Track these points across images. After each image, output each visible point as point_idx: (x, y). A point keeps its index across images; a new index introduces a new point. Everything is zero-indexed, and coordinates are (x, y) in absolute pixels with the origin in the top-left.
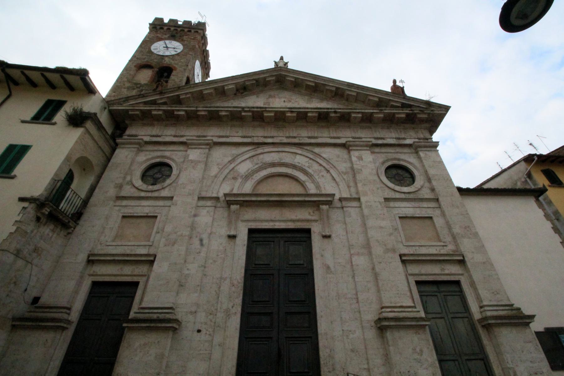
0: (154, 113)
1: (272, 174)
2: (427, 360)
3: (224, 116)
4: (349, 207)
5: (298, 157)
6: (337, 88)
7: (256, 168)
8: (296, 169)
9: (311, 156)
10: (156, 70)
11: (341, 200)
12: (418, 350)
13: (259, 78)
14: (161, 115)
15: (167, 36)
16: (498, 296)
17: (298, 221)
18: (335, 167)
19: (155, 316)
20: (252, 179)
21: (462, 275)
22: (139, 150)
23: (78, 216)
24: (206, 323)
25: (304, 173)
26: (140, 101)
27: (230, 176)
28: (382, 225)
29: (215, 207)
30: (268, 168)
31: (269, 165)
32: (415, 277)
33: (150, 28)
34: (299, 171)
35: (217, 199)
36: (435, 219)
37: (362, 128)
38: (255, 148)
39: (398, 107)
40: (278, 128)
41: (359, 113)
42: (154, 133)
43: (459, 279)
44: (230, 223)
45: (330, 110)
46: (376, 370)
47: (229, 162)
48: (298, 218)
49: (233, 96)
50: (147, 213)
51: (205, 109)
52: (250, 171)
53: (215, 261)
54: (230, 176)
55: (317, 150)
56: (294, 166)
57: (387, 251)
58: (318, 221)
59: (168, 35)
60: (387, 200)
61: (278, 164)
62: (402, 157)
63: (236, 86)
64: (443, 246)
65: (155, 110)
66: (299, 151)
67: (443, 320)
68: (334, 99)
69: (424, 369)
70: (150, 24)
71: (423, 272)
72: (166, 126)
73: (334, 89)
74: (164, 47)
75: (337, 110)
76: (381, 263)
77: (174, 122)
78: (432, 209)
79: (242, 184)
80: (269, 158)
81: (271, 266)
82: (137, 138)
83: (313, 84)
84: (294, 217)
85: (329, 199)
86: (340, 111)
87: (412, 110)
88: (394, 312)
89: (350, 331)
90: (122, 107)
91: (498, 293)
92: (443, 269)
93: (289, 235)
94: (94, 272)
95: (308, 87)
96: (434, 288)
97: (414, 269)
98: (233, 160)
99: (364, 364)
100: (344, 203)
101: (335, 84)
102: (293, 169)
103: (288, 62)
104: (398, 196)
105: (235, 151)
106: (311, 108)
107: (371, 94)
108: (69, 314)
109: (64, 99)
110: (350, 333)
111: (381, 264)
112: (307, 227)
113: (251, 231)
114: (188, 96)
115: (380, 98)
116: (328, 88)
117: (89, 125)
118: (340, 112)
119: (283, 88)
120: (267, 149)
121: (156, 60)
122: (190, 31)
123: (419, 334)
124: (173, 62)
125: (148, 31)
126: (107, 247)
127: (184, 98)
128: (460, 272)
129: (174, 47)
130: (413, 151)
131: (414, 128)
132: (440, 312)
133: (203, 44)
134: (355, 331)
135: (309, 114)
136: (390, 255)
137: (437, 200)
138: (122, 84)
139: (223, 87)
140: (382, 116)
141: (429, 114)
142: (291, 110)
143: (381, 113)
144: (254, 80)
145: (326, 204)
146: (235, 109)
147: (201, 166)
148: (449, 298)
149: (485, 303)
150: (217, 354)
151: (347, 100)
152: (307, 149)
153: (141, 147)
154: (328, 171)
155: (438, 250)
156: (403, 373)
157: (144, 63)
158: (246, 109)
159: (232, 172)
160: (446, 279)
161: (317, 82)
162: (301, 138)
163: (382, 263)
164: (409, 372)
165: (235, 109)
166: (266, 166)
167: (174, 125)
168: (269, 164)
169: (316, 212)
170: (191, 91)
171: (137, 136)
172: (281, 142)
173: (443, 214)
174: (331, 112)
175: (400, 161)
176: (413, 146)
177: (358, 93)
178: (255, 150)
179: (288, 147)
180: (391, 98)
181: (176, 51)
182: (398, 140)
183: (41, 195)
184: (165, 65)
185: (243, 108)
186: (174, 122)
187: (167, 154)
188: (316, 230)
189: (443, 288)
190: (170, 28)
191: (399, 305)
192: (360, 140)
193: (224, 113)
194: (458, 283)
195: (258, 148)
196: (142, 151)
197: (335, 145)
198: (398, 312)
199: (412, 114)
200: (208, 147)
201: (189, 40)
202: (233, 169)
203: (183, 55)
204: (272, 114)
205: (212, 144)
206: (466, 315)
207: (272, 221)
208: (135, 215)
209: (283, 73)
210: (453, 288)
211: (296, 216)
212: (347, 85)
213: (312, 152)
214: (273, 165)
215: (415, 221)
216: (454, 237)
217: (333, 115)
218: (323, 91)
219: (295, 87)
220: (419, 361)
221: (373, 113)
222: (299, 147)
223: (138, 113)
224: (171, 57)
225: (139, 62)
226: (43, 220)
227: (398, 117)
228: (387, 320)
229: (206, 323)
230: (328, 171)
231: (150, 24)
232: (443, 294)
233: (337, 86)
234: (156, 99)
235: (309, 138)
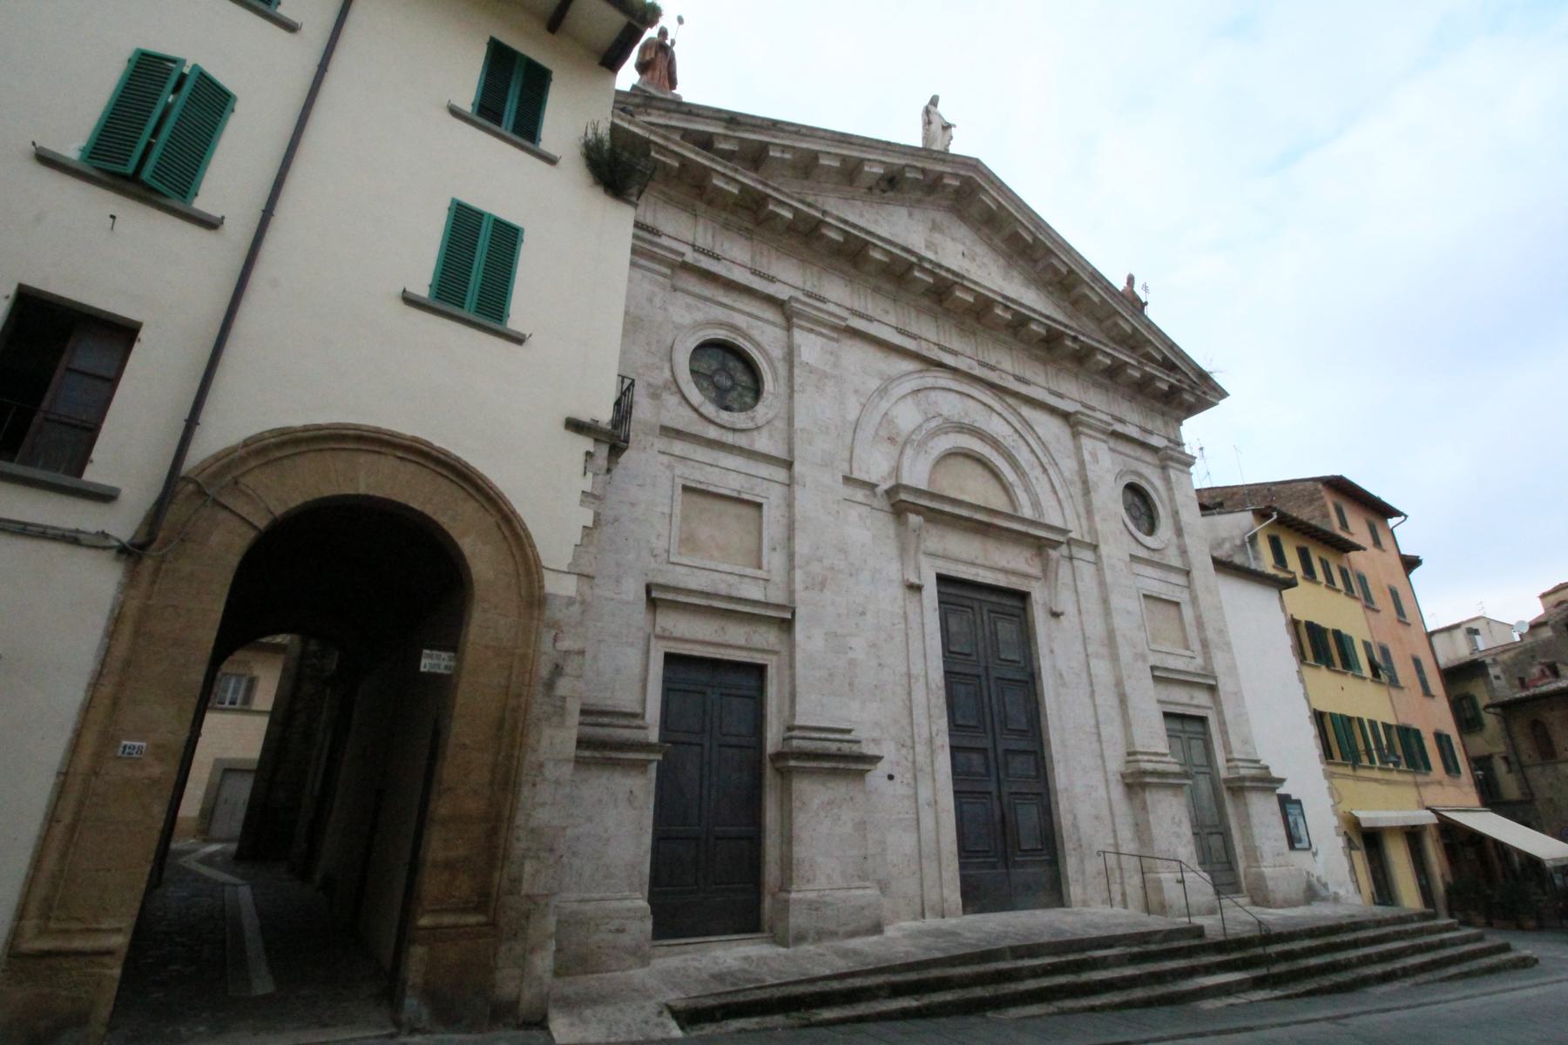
0: (718, 182)
5: (996, 419)
8: (997, 450)
9: (1018, 426)
12: (1177, 820)
18: (1056, 464)
19: (833, 747)
21: (1210, 708)
24: (898, 764)
26: (673, 123)
30: (952, 432)
35: (872, 486)
36: (1183, 607)
38: (921, 371)
40: (961, 330)
41: (1108, 355)
44: (903, 551)
49: (865, 190)
50: (739, 492)
51: (842, 226)
55: (1026, 411)
56: (995, 443)
60: (1133, 558)
61: (968, 429)
65: (723, 175)
66: (997, 406)
68: (1050, 289)
71: (1171, 699)
72: (726, 226)
73: (1064, 270)
82: (656, 239)
83: (1029, 239)
88: (1151, 761)
92: (1192, 698)
93: (994, 598)
94: (664, 630)
98: (882, 392)
103: (955, 126)
106: (1041, 314)
112: (1024, 588)
115: (1135, 329)
116: (1055, 262)
118: (1082, 341)
119: (960, 211)
120: (944, 380)
126: (671, 567)
127: (776, 158)
130: (1157, 462)
131: (1163, 414)
136: (1140, 664)
137: (1188, 573)
140: (1137, 374)
143: (1139, 368)
146: (904, 255)
149: (1236, 755)
151: (1074, 303)
154: (1045, 470)
158: (927, 265)
160: (1193, 713)
165: (904, 255)
167: (748, 234)
169: (1037, 561)
171: (660, 236)
173: (1194, 601)
174: (1068, 335)
176: (1161, 453)
178: (921, 375)
179: (978, 386)
185: (921, 258)
186: (746, 224)
187: (740, 321)
188: (1038, 595)
191: (1153, 750)
193: (877, 255)
194: (1202, 720)
195: (927, 370)
197: (1053, 411)
198: (1156, 762)
206: (1208, 770)
207: (973, 564)
208: (712, 489)
209: (978, 179)
210: (1197, 727)
211: (1008, 562)
214: (995, 444)
216: (1205, 644)
217: (1069, 343)
218: (1036, 261)
221: (1127, 363)
230: (1045, 470)
232: (1187, 735)
233: (1073, 267)
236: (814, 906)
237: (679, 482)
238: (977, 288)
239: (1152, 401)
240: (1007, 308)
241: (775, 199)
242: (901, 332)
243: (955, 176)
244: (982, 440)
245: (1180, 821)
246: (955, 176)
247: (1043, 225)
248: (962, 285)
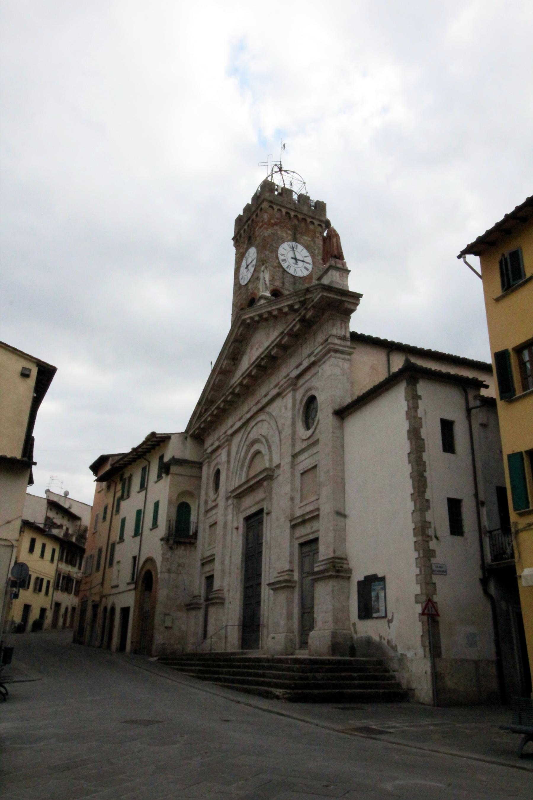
23: (195, 535)
38: (245, 429)
75: (262, 356)
79: (240, 475)
109: (162, 454)
117: (173, 469)
139: (221, 368)
141: (313, 306)
144: (232, 343)
183: (165, 534)
195: (247, 426)
200: (227, 443)
205: (230, 438)
224: (252, 279)
226: (174, 547)
240: (244, 378)
243: (239, 329)
246: (239, 327)
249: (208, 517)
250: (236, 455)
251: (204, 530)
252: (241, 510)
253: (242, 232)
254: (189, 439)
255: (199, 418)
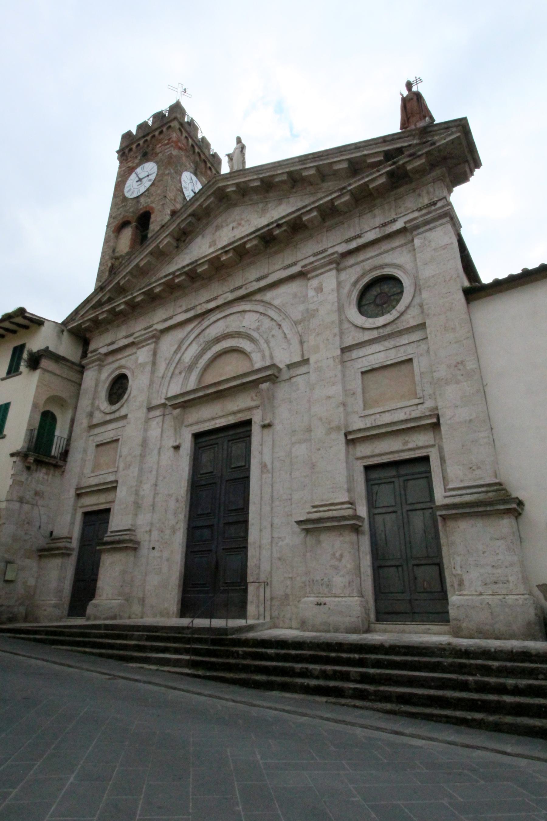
1: (217, 354)
2: (345, 566)
3: (160, 291)
4: (298, 375)
6: (290, 174)
7: (199, 352)
8: (242, 338)
10: (134, 224)
11: (289, 366)
12: (337, 555)
13: (194, 211)
14: (106, 317)
15: (137, 161)
16: (477, 472)
17: (239, 411)
20: (197, 368)
22: (101, 367)
23: (65, 454)
25: (250, 340)
26: (87, 309)
27: (177, 371)
28: (330, 393)
29: (164, 415)
31: (213, 343)
32: (365, 461)
33: (118, 159)
34: (245, 338)
37: (329, 229)
38: (200, 322)
39: (379, 163)
42: (108, 341)
43: (428, 454)
45: (271, 227)
46: (298, 579)
47: (175, 352)
48: (240, 408)
49: (176, 250)
52: (193, 358)
53: (165, 478)
54: (177, 371)
57: (330, 431)
58: (259, 406)
59: (139, 158)
62: (387, 259)
63: (173, 237)
64: (417, 405)
67: (393, 516)
68: (294, 190)
69: (341, 576)
70: (118, 152)
71: (377, 451)
73: (285, 177)
74: (137, 181)
75: (280, 222)
76: (319, 449)
77: (123, 319)
78: (414, 345)
79: (186, 378)
80: (214, 331)
81: (214, 473)
84: (235, 408)
85: (269, 373)
86: (284, 221)
87: (394, 163)
88: (320, 512)
89: (280, 538)
90: (75, 323)
91: (479, 468)
93: (231, 433)
95: (255, 190)
96: (392, 472)
97: (364, 450)
99: (289, 573)
100: (293, 372)
101: (284, 169)
102: (238, 337)
104: (368, 336)
105: (179, 334)
107: (335, 160)
108: (71, 542)
110: (280, 540)
111: (319, 452)
113: (197, 436)
114: (127, 279)
115: (349, 160)
117: (45, 363)
118: (285, 222)
120: (213, 317)
121: (131, 210)
122: (161, 132)
123: (343, 536)
124: (149, 200)
125: (117, 163)
128: (432, 442)
129: (147, 174)
132: (394, 504)
133: (186, 137)
134: (285, 537)
135: (248, 246)
136: (334, 436)
138: (105, 266)
139: (158, 246)
140: (346, 198)
142: (225, 250)
144: (189, 215)
145: (265, 381)
147: (149, 368)
148: (410, 483)
150: (165, 569)
152: (256, 300)
153: (103, 361)
155: (408, 413)
156: (317, 581)
157: (121, 222)
158: (177, 273)
159: (178, 366)
161: (263, 177)
162: (248, 286)
163: (321, 449)
164: (322, 580)
166: (210, 345)
167: (124, 322)
168: (212, 341)
170: (127, 271)
172: (226, 301)
174: (273, 228)
175: (383, 268)
177: (318, 168)
179: (236, 305)
180: (365, 152)
181: (150, 180)
182: (383, 228)
183: (23, 447)
184: (142, 212)
185: (173, 273)
186: (123, 319)
188: (257, 418)
189: (404, 470)
190: (138, 143)
192: (324, 255)
195: (203, 320)
196: (104, 366)
198: (324, 511)
199: (398, 168)
200: (154, 340)
201: (163, 148)
202: (180, 359)
203: (159, 181)
204: (206, 267)
205: (158, 334)
208: (104, 441)
211: (238, 406)
212: (299, 161)
213: (262, 301)
215: (386, 373)
219: (243, 196)
220: (336, 568)
221: (332, 200)
222: (247, 301)
223: (88, 324)
224: (146, 193)
225: (117, 222)
226: (33, 467)
227: (373, 188)
228: (303, 523)
229: (158, 541)
231: (118, 152)
232: (402, 479)
233: (287, 170)
234: (100, 299)
235: (258, 280)
236: (96, 606)
237: (94, 444)
238: (206, 259)
239: (392, 193)
240: (226, 252)
241: (116, 306)
242: (186, 311)
243: (208, 197)
244: (232, 338)
245: (341, 556)
246: (208, 197)
247: (259, 169)
248: (199, 265)
249: (91, 434)
250: (173, 355)
251: (85, 451)
252: (186, 423)
253: (134, 146)
254: (65, 333)
255: (94, 307)
